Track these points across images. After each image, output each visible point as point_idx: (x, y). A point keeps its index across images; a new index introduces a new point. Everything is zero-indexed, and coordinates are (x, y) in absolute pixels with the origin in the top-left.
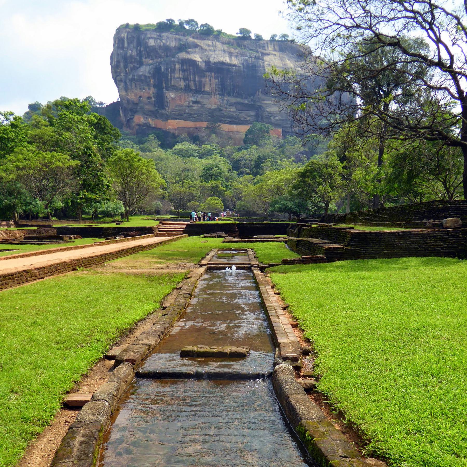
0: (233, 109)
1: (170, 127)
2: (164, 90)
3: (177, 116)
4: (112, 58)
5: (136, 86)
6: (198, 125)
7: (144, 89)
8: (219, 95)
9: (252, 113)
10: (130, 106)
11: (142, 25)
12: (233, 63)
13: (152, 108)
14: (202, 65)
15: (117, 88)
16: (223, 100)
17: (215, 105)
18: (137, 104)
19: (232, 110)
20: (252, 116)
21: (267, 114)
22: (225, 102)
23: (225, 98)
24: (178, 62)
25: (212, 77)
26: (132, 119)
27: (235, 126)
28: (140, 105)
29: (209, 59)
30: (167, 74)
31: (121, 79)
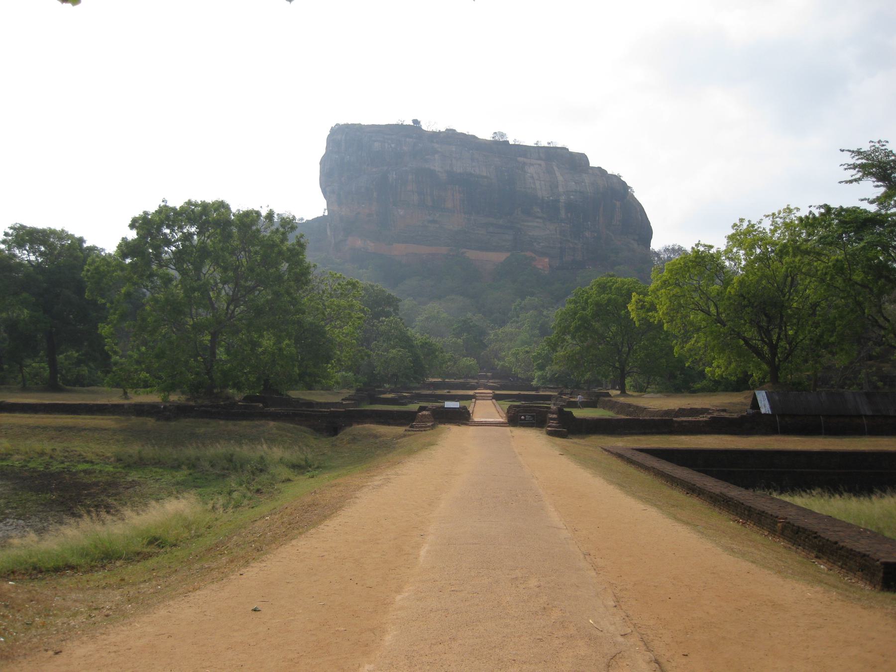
12: (485, 174)
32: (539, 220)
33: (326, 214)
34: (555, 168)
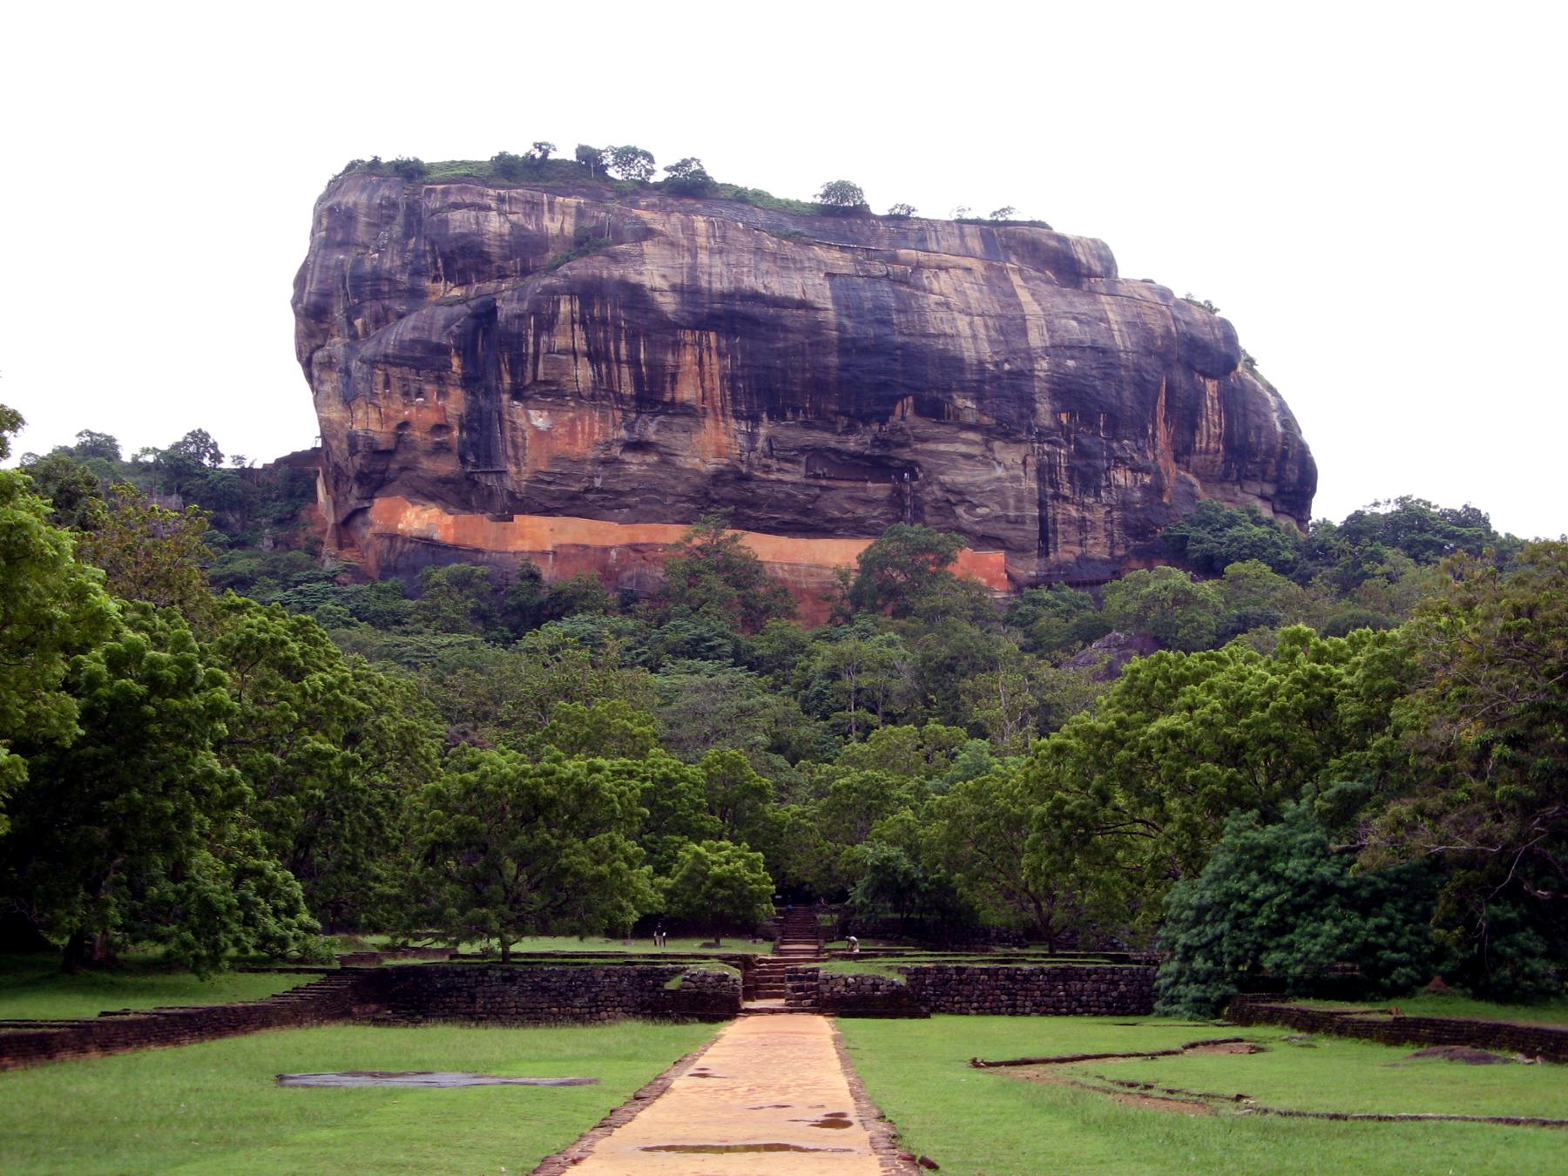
0: (794, 474)
1: (524, 545)
2: (505, 397)
3: (555, 499)
4: (300, 281)
5: (387, 384)
6: (643, 539)
7: (420, 393)
8: (738, 416)
9: (878, 490)
10: (358, 460)
11: (432, 165)
13: (447, 466)
14: (668, 303)
15: (309, 395)
16: (752, 437)
17: (719, 454)
18: (388, 453)
19: (787, 478)
20: (876, 501)
21: (939, 494)
24: (572, 294)
25: (709, 348)
26: (364, 511)
27: (802, 543)
28: (399, 457)
29: (694, 278)
30: (520, 338)
31: (330, 357)
32: (971, 436)
33: (319, 445)
34: (1016, 279)
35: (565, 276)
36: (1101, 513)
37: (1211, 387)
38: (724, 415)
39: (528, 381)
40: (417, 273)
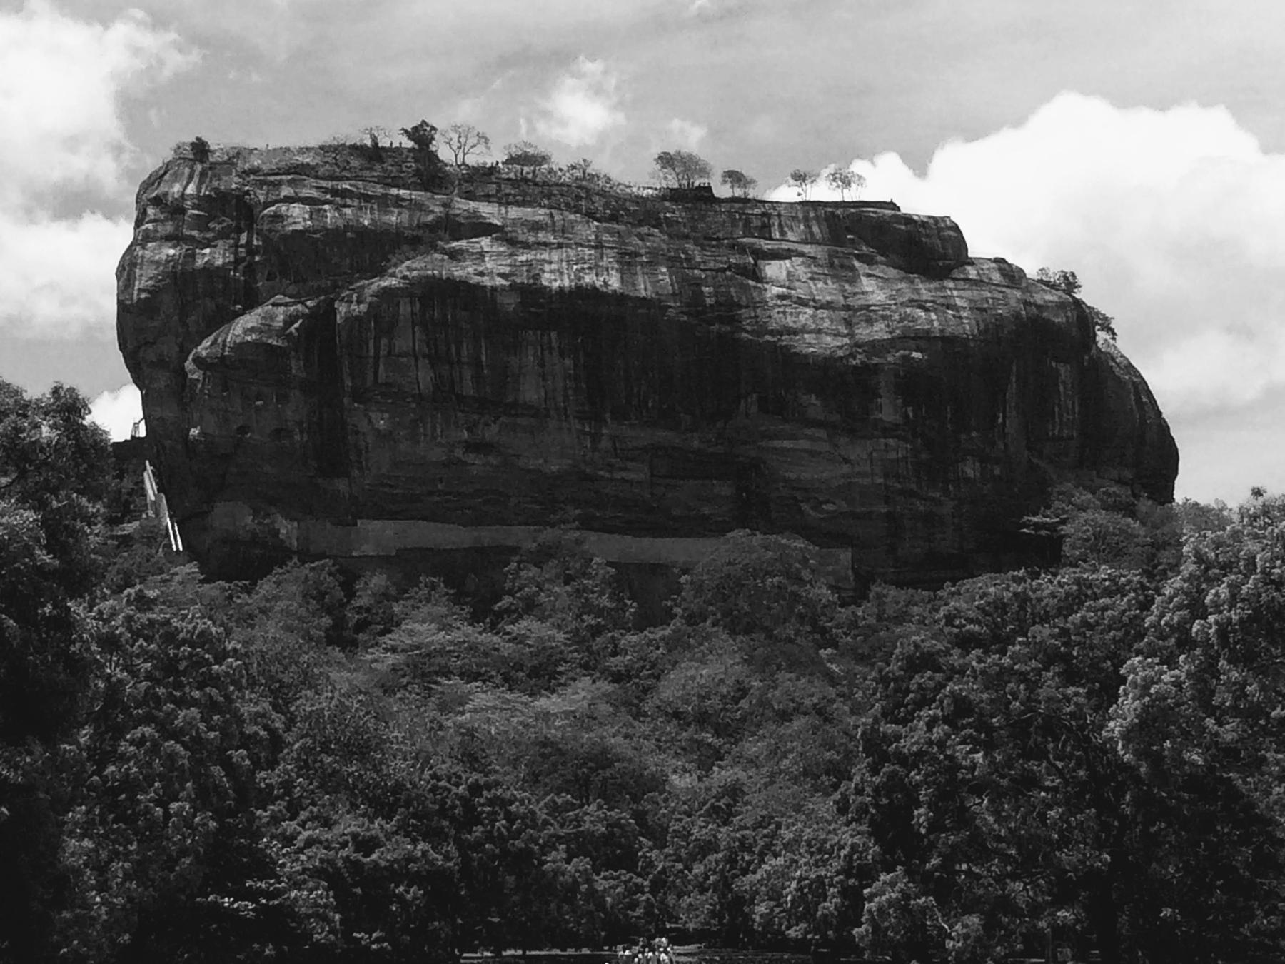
0: (637, 473)
1: (368, 549)
9: (725, 489)
14: (510, 302)
16: (596, 438)
19: (632, 476)
22: (605, 444)
23: (604, 431)
25: (551, 348)
27: (646, 541)
29: (537, 277)
33: (142, 433)
35: (405, 277)
36: (948, 508)
37: (1064, 370)
38: (567, 416)
39: (369, 384)
40: (250, 270)
